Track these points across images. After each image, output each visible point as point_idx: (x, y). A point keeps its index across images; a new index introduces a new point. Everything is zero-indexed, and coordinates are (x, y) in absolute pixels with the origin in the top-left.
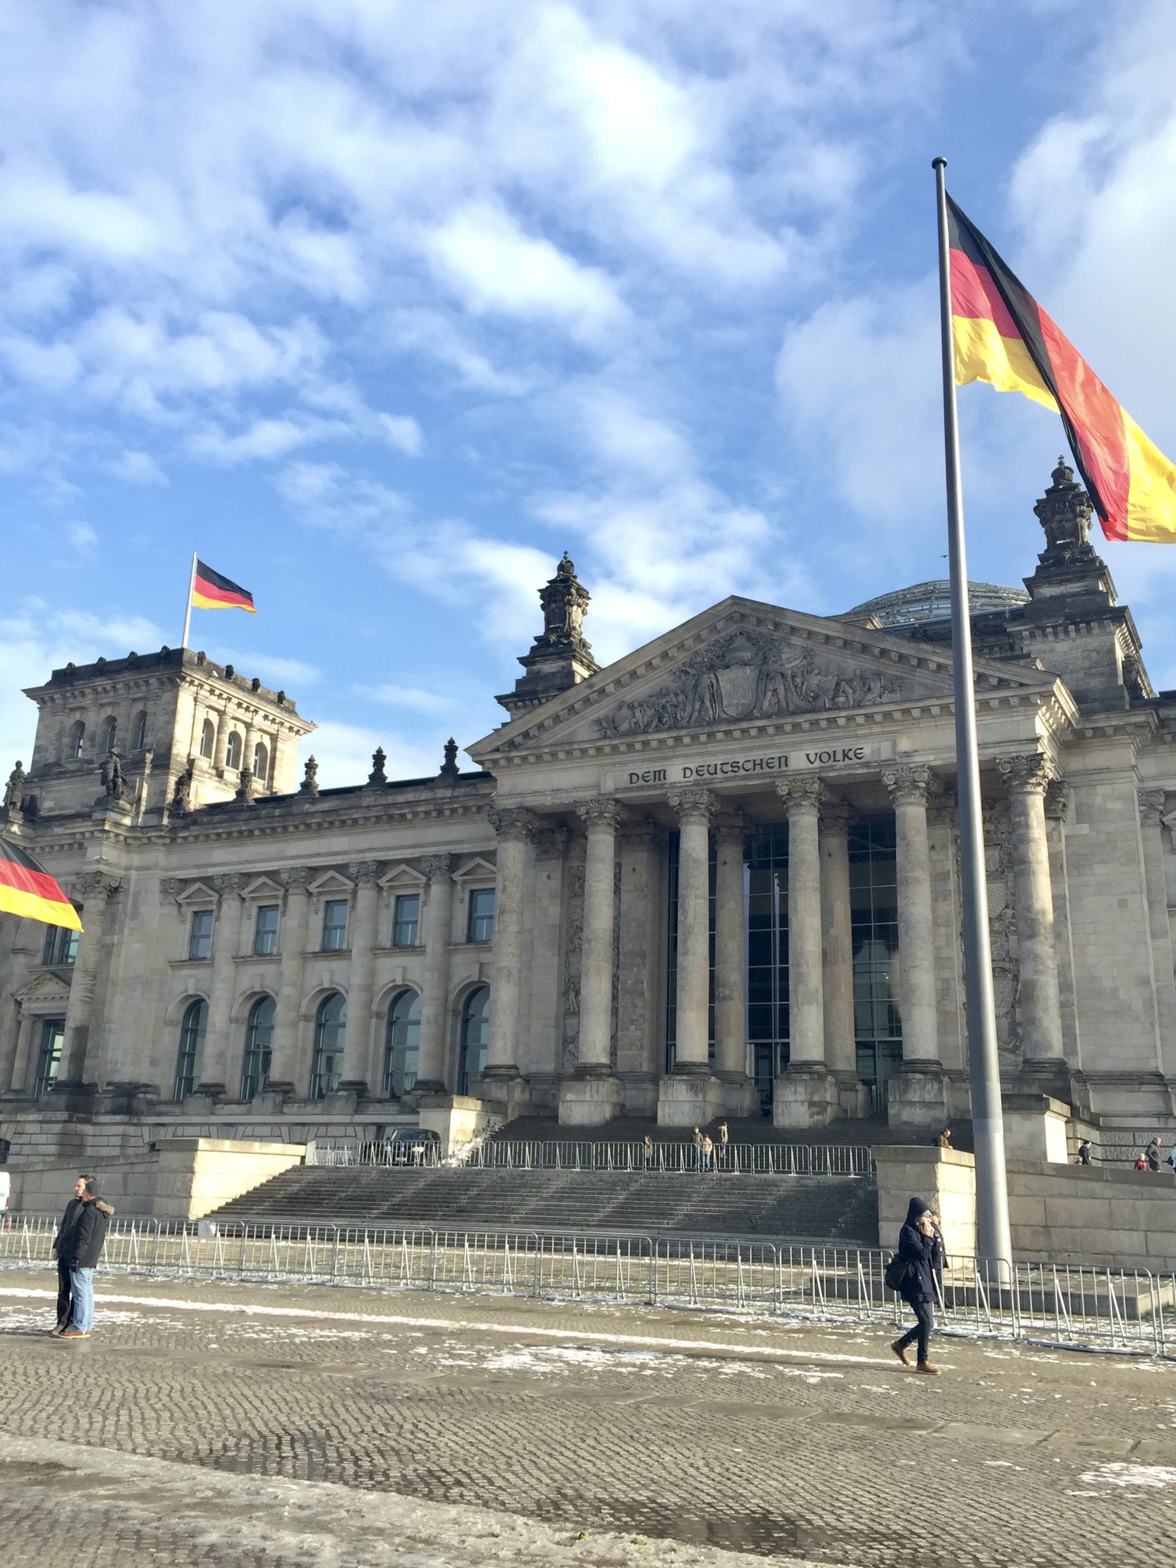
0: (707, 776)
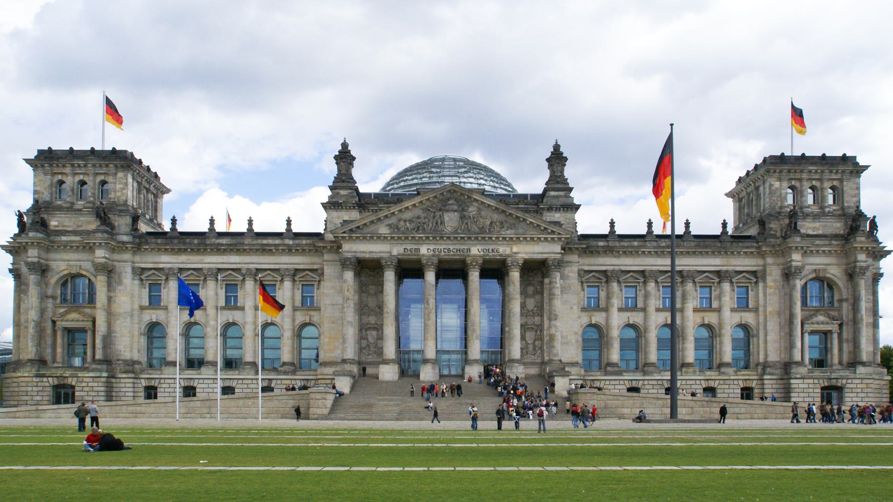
0: (437, 253)
